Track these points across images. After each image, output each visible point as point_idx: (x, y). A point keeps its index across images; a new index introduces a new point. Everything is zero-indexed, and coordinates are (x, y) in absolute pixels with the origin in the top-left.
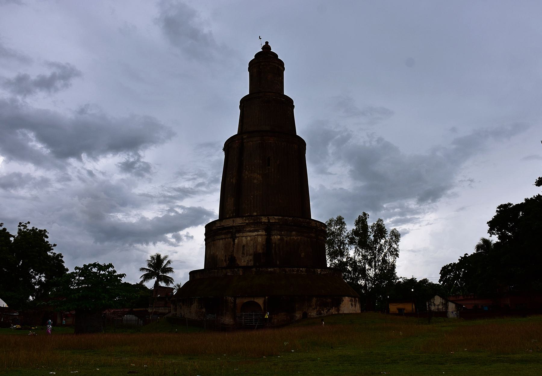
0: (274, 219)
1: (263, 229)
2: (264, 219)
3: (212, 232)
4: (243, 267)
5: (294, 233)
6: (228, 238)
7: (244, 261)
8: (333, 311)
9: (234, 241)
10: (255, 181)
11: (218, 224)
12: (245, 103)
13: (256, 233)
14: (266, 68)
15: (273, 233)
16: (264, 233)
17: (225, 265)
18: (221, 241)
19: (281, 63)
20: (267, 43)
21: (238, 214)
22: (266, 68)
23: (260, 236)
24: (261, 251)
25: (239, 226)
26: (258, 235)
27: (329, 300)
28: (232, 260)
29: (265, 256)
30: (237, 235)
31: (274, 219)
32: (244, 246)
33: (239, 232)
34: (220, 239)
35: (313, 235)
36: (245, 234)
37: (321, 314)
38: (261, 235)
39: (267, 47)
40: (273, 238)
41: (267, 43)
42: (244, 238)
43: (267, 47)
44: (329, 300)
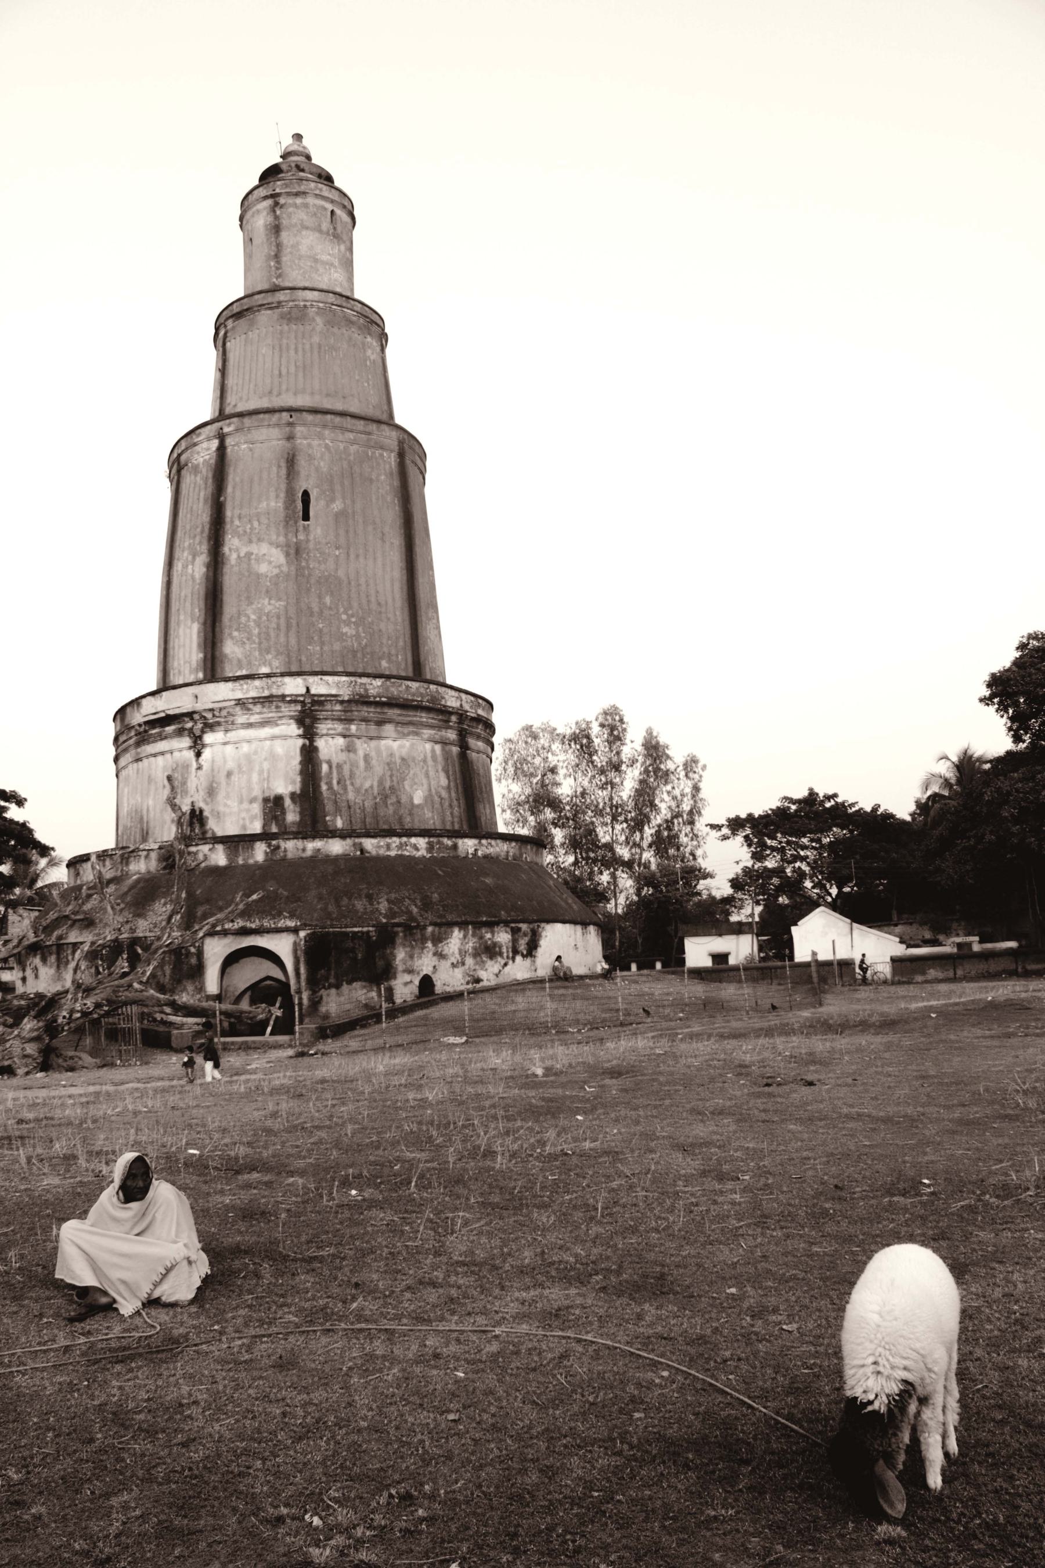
1: (291, 717)
2: (294, 686)
4: (225, 840)
6: (180, 751)
9: (198, 755)
10: (263, 568)
11: (151, 708)
13: (267, 731)
16: (293, 729)
18: (160, 758)
21: (212, 669)
25: (212, 710)
26: (273, 738)
30: (208, 738)
31: (320, 687)
32: (229, 774)
34: (155, 755)
36: (232, 735)
38: (285, 737)
40: (320, 743)
41: (298, 137)
42: (229, 749)
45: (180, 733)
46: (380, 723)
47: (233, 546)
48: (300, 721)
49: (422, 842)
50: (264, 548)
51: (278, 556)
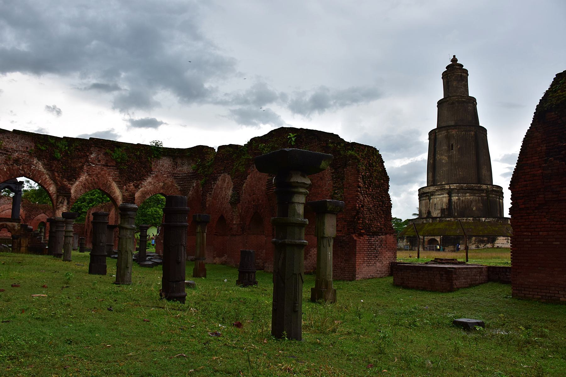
0: (452, 187)
2: (447, 187)
3: (422, 194)
5: (468, 194)
7: (436, 213)
8: (489, 245)
10: (443, 161)
12: (440, 104)
13: (442, 196)
14: (455, 75)
15: (453, 195)
16: (447, 195)
17: (425, 216)
19: (466, 71)
20: (454, 56)
22: (455, 75)
23: (444, 198)
24: (445, 207)
27: (485, 239)
28: (429, 213)
29: (448, 211)
31: (452, 187)
33: (432, 195)
35: (484, 195)
36: (436, 197)
37: (478, 247)
39: (454, 60)
40: (452, 198)
41: (454, 56)
43: (454, 60)
44: (485, 239)
45: (427, 196)
46: (466, 194)
47: (438, 157)
48: (448, 194)
49: (471, 219)
50: (444, 157)
51: (446, 158)
